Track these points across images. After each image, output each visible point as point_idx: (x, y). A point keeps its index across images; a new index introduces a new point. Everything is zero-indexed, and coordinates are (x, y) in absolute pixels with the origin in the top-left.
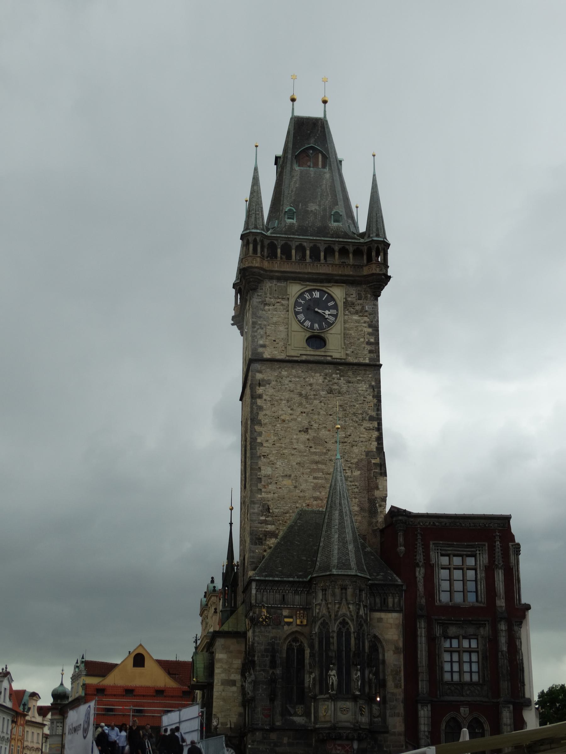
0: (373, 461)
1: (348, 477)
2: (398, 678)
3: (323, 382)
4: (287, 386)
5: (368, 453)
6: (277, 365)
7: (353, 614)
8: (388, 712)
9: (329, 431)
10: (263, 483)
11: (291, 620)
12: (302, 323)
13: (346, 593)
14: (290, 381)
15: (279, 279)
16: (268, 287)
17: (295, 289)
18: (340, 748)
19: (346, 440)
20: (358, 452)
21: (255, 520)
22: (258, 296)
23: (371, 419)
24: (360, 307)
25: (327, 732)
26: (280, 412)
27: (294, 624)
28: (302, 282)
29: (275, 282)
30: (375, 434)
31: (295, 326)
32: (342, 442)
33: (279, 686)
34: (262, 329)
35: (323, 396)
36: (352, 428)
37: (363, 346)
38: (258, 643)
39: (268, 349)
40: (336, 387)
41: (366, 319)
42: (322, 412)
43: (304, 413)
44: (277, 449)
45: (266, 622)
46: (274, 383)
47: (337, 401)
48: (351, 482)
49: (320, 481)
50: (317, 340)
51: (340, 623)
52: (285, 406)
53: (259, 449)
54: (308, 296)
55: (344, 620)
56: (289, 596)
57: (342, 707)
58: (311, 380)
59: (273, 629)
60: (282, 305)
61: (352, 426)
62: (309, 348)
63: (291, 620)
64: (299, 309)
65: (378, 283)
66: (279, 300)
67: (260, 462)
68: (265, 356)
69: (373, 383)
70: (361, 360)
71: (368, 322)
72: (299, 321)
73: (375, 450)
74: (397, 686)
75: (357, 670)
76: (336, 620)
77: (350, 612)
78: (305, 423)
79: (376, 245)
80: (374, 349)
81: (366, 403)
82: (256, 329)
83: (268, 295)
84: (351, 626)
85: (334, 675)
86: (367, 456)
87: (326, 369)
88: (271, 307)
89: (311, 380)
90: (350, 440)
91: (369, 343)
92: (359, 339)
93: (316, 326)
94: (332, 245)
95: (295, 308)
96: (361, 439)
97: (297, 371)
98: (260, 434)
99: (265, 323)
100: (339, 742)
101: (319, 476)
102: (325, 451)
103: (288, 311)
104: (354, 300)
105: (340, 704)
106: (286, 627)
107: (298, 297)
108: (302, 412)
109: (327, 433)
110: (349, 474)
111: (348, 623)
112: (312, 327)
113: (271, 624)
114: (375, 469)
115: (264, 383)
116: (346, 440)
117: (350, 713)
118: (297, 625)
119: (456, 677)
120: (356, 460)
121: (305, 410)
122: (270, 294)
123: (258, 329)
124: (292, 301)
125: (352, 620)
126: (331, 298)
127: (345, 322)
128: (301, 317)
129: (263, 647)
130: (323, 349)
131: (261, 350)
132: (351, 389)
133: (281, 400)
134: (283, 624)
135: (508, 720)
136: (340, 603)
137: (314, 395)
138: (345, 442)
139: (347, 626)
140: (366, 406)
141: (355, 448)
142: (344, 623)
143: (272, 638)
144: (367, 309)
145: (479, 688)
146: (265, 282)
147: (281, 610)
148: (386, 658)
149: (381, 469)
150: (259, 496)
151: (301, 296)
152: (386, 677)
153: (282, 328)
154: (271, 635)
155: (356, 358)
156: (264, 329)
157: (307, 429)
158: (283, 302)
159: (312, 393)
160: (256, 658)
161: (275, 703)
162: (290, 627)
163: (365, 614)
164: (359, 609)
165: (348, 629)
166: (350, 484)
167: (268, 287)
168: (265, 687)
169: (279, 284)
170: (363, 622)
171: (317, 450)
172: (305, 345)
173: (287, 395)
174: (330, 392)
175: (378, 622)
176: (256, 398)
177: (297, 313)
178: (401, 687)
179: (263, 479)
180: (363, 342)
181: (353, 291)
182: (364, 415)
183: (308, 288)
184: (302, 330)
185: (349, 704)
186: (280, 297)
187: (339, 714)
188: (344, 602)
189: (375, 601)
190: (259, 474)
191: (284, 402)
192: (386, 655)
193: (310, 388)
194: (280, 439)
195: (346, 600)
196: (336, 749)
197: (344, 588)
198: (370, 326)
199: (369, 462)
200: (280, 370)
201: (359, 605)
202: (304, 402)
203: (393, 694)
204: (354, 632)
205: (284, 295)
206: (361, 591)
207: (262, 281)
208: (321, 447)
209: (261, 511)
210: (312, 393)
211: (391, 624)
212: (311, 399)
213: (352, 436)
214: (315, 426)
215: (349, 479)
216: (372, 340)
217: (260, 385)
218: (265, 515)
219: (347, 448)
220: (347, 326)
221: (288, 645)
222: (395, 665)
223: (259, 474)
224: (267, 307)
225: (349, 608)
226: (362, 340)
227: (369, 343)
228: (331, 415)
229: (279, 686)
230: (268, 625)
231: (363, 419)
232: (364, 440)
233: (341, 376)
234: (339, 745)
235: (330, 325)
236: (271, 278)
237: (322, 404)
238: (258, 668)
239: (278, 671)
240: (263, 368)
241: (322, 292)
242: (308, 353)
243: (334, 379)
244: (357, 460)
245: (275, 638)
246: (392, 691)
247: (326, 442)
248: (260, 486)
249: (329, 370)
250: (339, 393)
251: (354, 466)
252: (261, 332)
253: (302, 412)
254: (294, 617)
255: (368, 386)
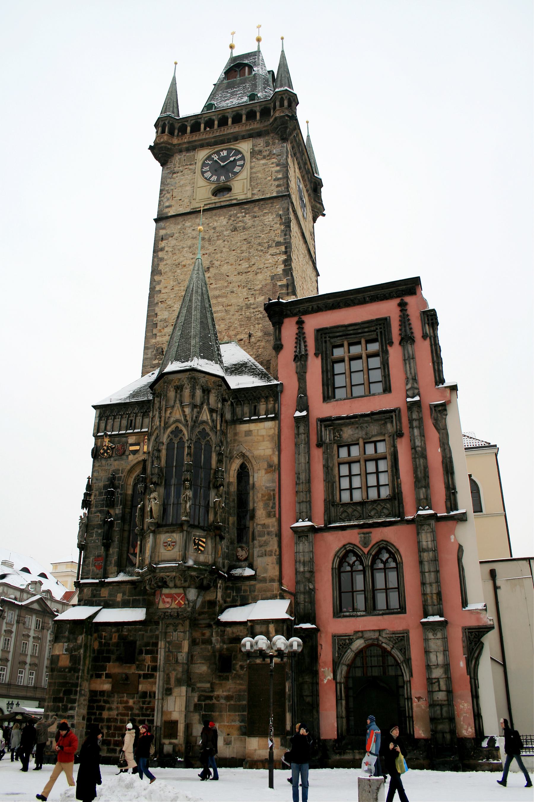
0: (279, 283)
1: (251, 304)
2: (271, 505)
3: (227, 223)
4: (190, 235)
5: (273, 278)
6: (180, 219)
7: (188, 418)
8: (256, 552)
9: (232, 265)
10: (159, 328)
11: (137, 448)
12: (208, 179)
13: (181, 396)
14: (193, 230)
15: (188, 150)
16: (177, 159)
17: (202, 154)
18: (169, 600)
19: (249, 269)
20: (261, 279)
21: (147, 366)
22: (168, 168)
23: (278, 244)
24: (268, 153)
25: (149, 577)
26: (182, 259)
27: (141, 452)
28: (209, 147)
29: (184, 153)
30: (284, 257)
31: (201, 182)
32: (245, 273)
33: (117, 529)
34: (168, 193)
35: (226, 235)
36: (256, 257)
37: (270, 183)
38: (97, 480)
39: (173, 208)
40: (241, 224)
41: (274, 160)
42: (224, 250)
43: (206, 254)
44: (176, 292)
45: (107, 453)
46: (176, 235)
47: (239, 237)
48: (254, 308)
49: (220, 314)
50: (222, 189)
51: (172, 432)
52: (187, 252)
53: (157, 297)
54: (215, 157)
55: (177, 427)
56: (138, 421)
57: (166, 541)
58: (215, 224)
59: (115, 460)
60: (190, 170)
61: (256, 256)
62: (213, 198)
63: (137, 448)
64: (205, 169)
65: (283, 126)
66: (187, 167)
67: (157, 309)
68: (170, 215)
69: (281, 212)
70: (268, 196)
71: (276, 162)
72: (206, 178)
73: (281, 272)
74: (269, 515)
75: (186, 489)
76: (166, 428)
77: (185, 416)
78: (206, 264)
79: (280, 97)
80: (282, 183)
81: (272, 231)
82: (163, 195)
83: (177, 165)
84: (186, 433)
85: (155, 499)
86: (272, 280)
87: (230, 211)
88: (178, 174)
89: (215, 224)
90: (254, 268)
91: (276, 179)
92: (266, 179)
93: (223, 178)
94: (240, 112)
95: (202, 168)
96: (266, 265)
97: (202, 219)
98: (159, 282)
99: (172, 188)
100: (165, 591)
101: (218, 309)
102: (226, 284)
103: (195, 173)
104: (261, 148)
105: (163, 537)
106: (131, 457)
107: (206, 160)
108: (204, 254)
109: (229, 267)
110: (252, 301)
111: (181, 431)
112: (218, 179)
113: (114, 455)
114: (280, 290)
115: (167, 237)
116: (249, 269)
117: (176, 549)
118: (144, 453)
119: (358, 496)
120: (260, 286)
121: (207, 252)
122: (179, 164)
123: (165, 194)
124: (199, 164)
125: (186, 425)
126: (238, 152)
127: (251, 168)
128: (208, 175)
129: (101, 484)
130: (228, 195)
131: (166, 210)
132: (257, 222)
133: (183, 248)
134: (127, 453)
135: (429, 543)
136: (173, 407)
137: (218, 236)
138: (249, 272)
139: (180, 435)
140: (272, 234)
141: (259, 275)
142: (177, 432)
143: (114, 471)
144: (274, 152)
145: (388, 506)
146: (175, 156)
147: (127, 437)
148: (255, 480)
149: (288, 290)
150: (154, 341)
151: (209, 158)
152: (255, 505)
153: (188, 188)
154: (113, 468)
155: (263, 195)
156: (171, 193)
157: (208, 268)
158: (191, 167)
159: (215, 235)
160: (93, 497)
161: (111, 551)
162: (137, 456)
163: (213, 421)
164: (199, 413)
165: (181, 438)
166: (252, 310)
167: (177, 159)
168: (100, 531)
169: (188, 154)
170: (208, 430)
171: (218, 285)
172: (210, 196)
173: (189, 243)
174: (235, 229)
175: (245, 436)
176: (158, 251)
177: (203, 173)
178: (275, 516)
179: (159, 325)
180: (269, 180)
181: (260, 142)
182: (270, 243)
183: (216, 150)
184: (208, 184)
185: (177, 537)
186: (188, 164)
187: (162, 550)
188: (178, 404)
189: (243, 411)
190: (155, 319)
191: (186, 249)
192: (256, 475)
193: (213, 231)
194: (179, 283)
195: (181, 403)
196: (164, 602)
197: (179, 389)
198: (277, 165)
199: (275, 285)
200: (183, 223)
201: (201, 407)
202: (207, 244)
203: (264, 525)
204: (188, 440)
205: (193, 162)
206: (206, 391)
207: (173, 156)
208: (221, 282)
209: (155, 355)
210: (215, 235)
211: (263, 436)
212: (214, 240)
213: (256, 265)
214: (217, 263)
215: (252, 306)
216: (280, 176)
217: (162, 239)
218: (158, 359)
219: (250, 277)
220: (254, 170)
221: (135, 479)
222: (266, 488)
223: (155, 319)
224: (175, 175)
225: (184, 412)
226: (270, 178)
227: (276, 179)
228: (233, 250)
229: (117, 529)
230: (110, 457)
231: (269, 247)
232: (269, 265)
233: (246, 214)
234: (168, 596)
235: (236, 174)
236: (181, 151)
237: (226, 242)
238: (93, 509)
239: (118, 511)
240: (168, 224)
241: (229, 150)
242: (213, 201)
243: (238, 218)
244: (261, 286)
245: (116, 471)
246: (263, 522)
247: (228, 276)
248: (155, 331)
249: (234, 211)
250: (244, 228)
251: (258, 292)
252: (168, 196)
253: (204, 254)
254: (142, 444)
255: (275, 216)
